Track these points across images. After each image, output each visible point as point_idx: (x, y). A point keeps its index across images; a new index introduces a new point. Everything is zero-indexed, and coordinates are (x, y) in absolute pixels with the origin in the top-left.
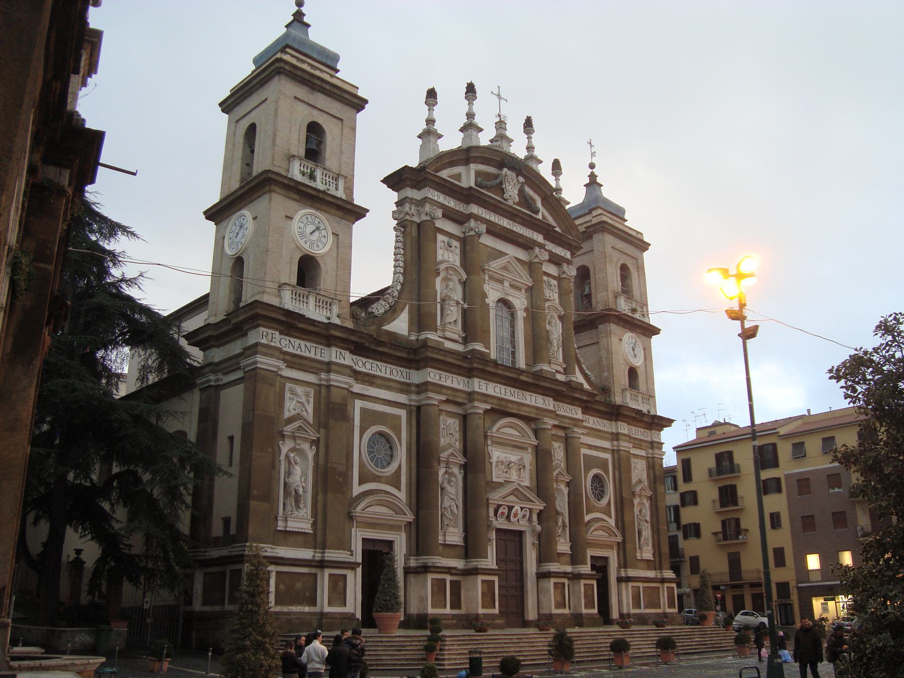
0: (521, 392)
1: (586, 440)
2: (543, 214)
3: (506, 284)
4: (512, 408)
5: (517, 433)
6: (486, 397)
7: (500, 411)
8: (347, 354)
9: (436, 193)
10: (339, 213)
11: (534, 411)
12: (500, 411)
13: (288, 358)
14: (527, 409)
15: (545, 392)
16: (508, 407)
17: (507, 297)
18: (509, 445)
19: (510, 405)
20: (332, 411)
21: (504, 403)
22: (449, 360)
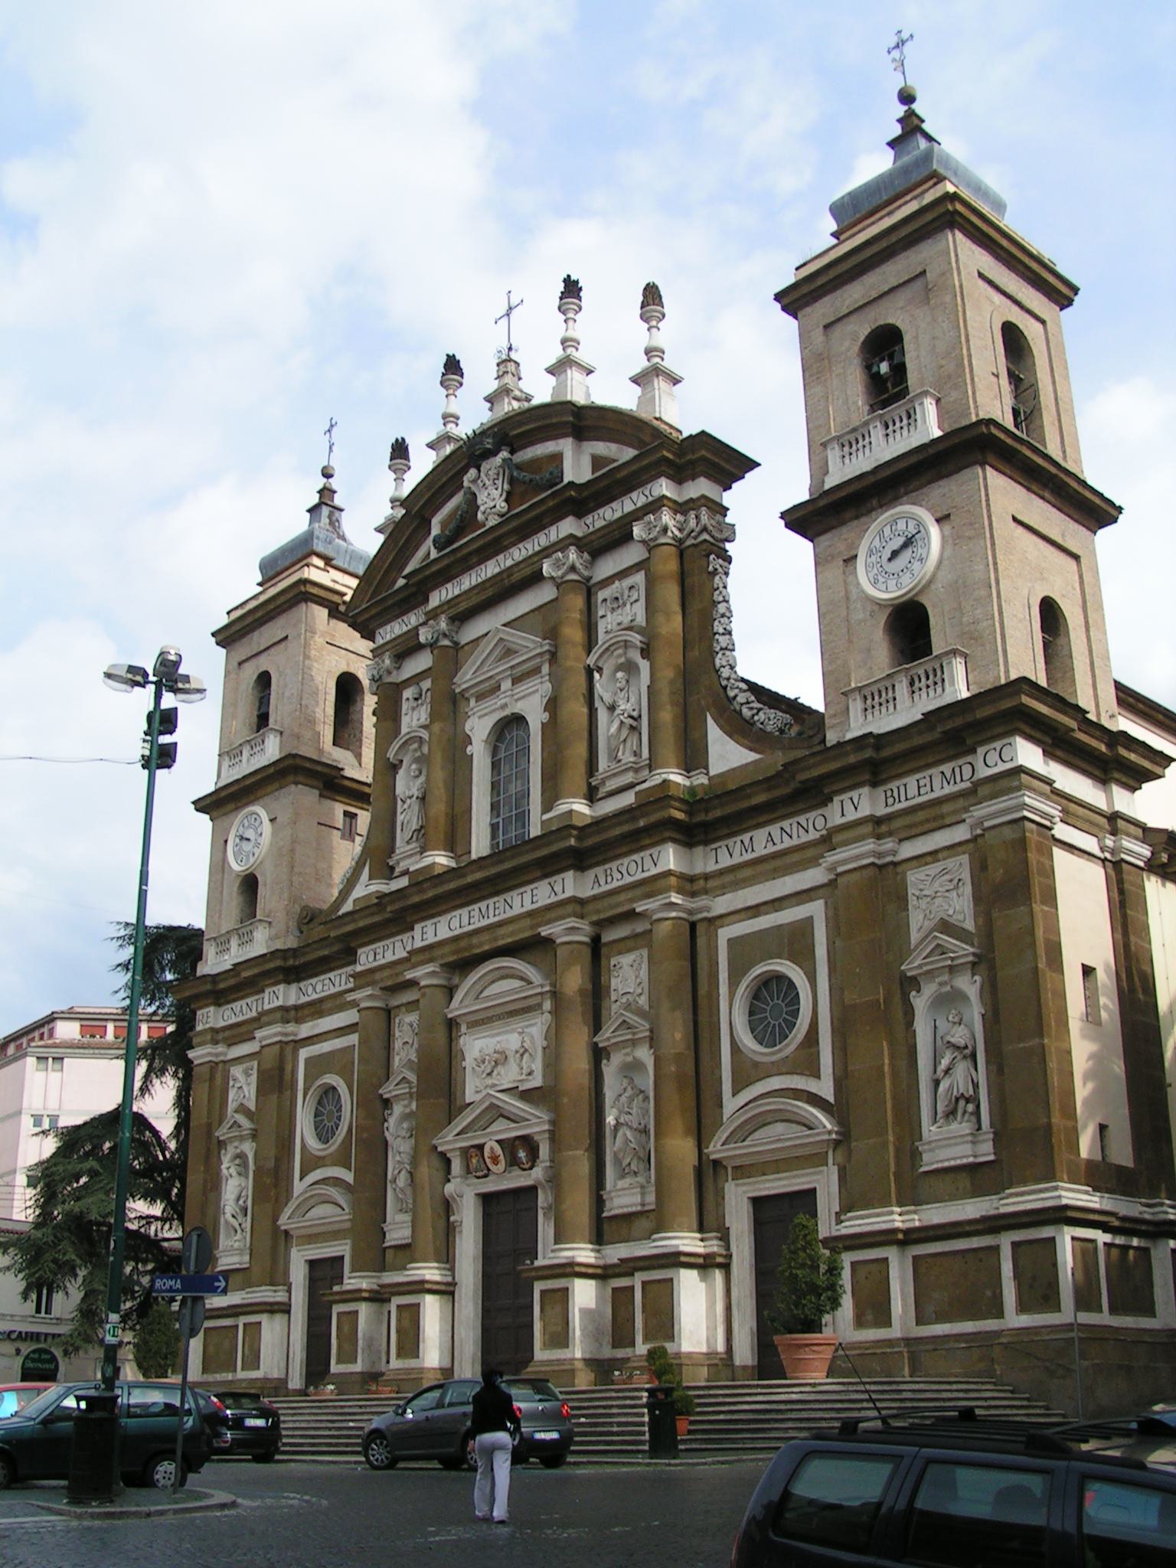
0: (500, 899)
1: (721, 904)
2: (576, 465)
3: (506, 685)
4: (481, 945)
5: (516, 984)
6: (426, 953)
7: (462, 960)
8: (281, 988)
9: (388, 627)
10: (276, 785)
11: (528, 922)
12: (462, 960)
13: (227, 1033)
14: (510, 928)
15: (548, 866)
16: (471, 947)
17: (507, 712)
18: (499, 1017)
19: (475, 940)
20: (275, 1080)
21: (463, 944)
22: (361, 924)
